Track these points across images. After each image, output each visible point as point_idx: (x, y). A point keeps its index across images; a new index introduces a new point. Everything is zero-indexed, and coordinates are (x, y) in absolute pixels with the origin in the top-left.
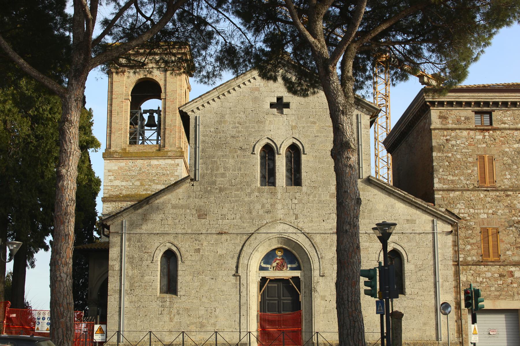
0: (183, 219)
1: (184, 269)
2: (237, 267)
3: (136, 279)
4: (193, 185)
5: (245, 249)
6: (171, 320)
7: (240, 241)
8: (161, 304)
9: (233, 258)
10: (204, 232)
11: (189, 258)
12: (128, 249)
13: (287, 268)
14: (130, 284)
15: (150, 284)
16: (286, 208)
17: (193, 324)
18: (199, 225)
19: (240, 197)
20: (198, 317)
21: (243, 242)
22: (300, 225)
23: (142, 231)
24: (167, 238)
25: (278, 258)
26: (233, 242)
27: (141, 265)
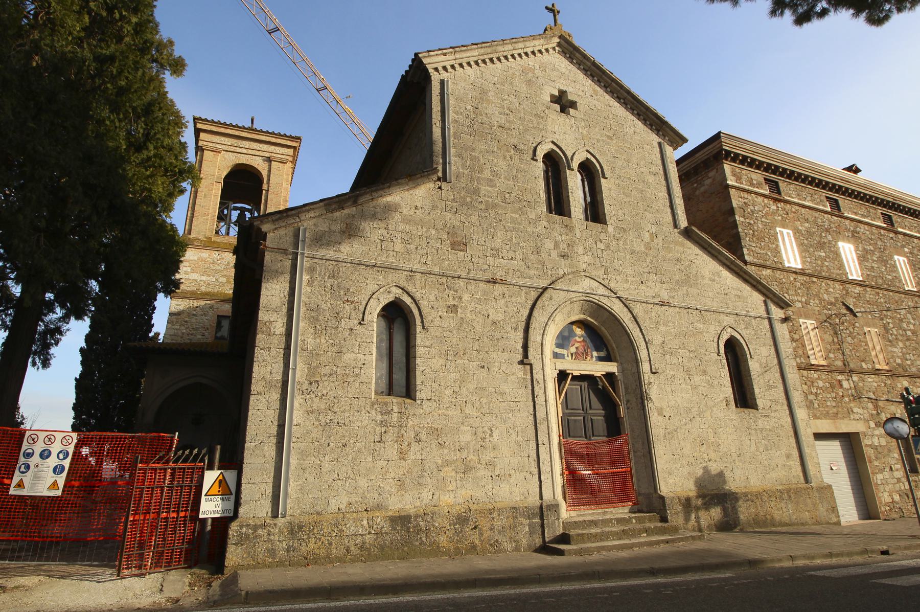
0: (425, 246)
1: (428, 344)
2: (525, 347)
3: (323, 359)
4: (440, 188)
5: (535, 313)
6: (402, 455)
7: (525, 299)
8: (379, 418)
9: (516, 329)
10: (464, 275)
11: (437, 321)
12: (309, 289)
13: (592, 357)
14: (309, 368)
15: (357, 370)
16: (590, 253)
17: (447, 463)
18: (452, 260)
19: (520, 224)
20: (458, 447)
21: (530, 303)
22: (612, 285)
23: (340, 256)
24: (392, 277)
25: (577, 339)
26: (513, 299)
27: (336, 328)
